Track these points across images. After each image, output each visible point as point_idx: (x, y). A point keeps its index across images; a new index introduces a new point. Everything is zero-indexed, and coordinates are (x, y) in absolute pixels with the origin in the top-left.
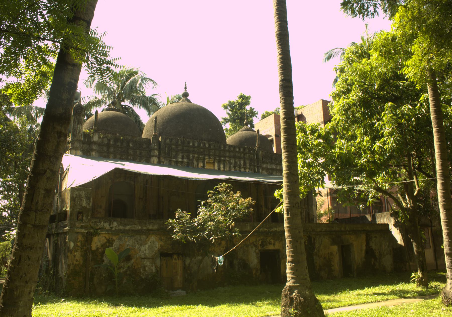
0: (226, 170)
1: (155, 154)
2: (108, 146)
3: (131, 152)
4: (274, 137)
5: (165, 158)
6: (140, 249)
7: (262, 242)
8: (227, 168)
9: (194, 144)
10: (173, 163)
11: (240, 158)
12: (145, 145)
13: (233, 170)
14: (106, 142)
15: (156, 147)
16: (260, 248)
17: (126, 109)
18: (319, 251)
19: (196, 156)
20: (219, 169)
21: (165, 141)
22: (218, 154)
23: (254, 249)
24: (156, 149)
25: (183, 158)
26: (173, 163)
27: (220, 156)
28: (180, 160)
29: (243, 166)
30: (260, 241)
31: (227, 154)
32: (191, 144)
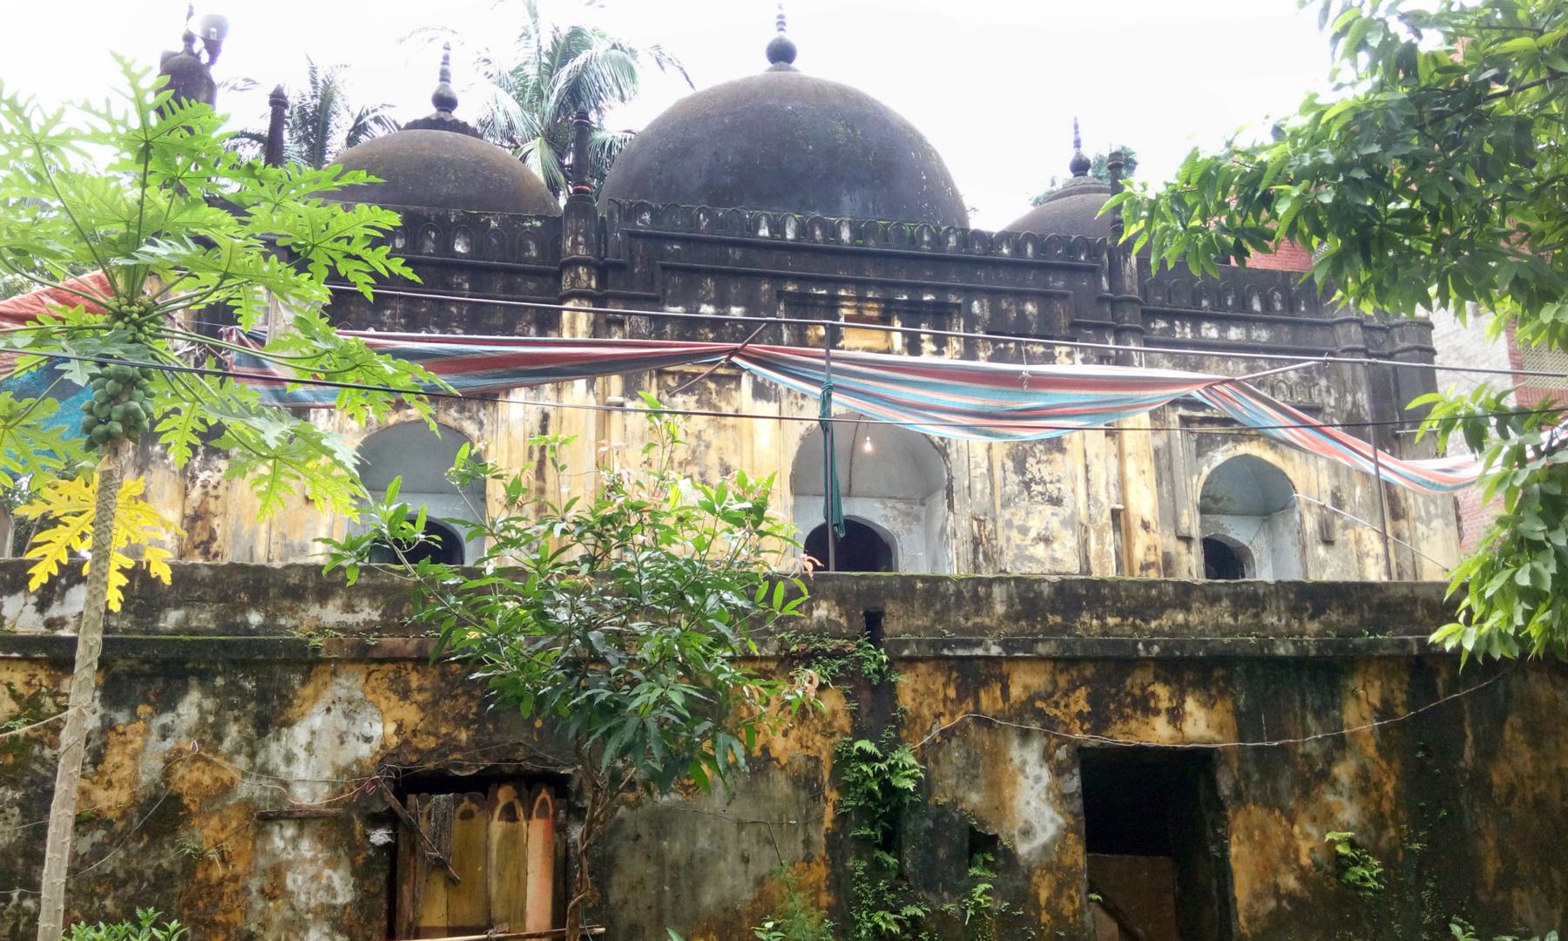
28: (707, 310)
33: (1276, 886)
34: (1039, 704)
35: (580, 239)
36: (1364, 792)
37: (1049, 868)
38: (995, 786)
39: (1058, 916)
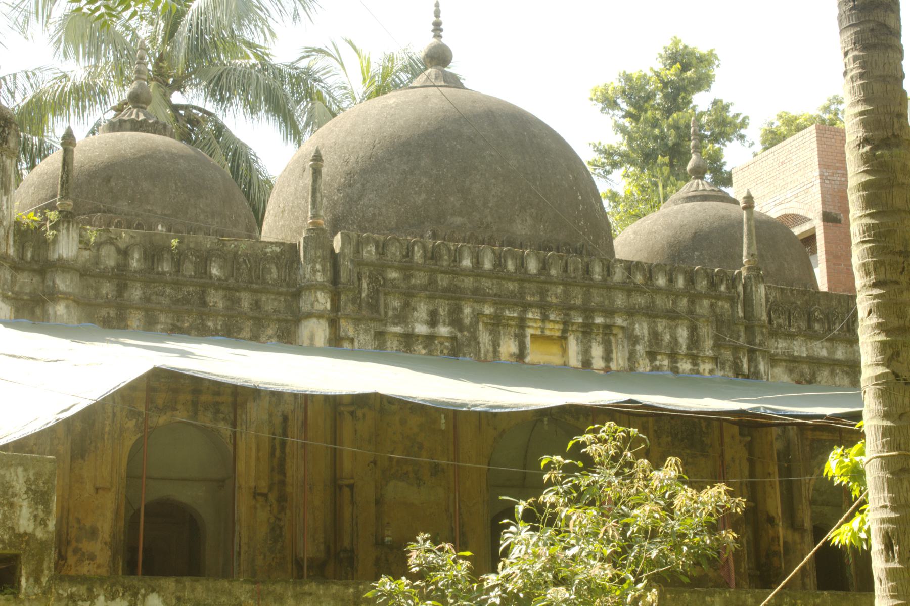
0: (613, 366)
1: (319, 307)
2: (121, 276)
3: (216, 299)
4: (817, 224)
5: (357, 321)
8: (619, 361)
9: (478, 263)
10: (392, 344)
11: (673, 316)
12: (274, 270)
13: (644, 365)
14: (111, 263)
15: (319, 277)
17: (188, 123)
19: (488, 310)
20: (587, 364)
21: (357, 251)
22: (579, 302)
24: (321, 287)
25: (433, 321)
26: (392, 344)
27: (588, 311)
28: (421, 329)
29: (689, 348)
31: (620, 300)
32: (467, 263)
35: (318, 267)
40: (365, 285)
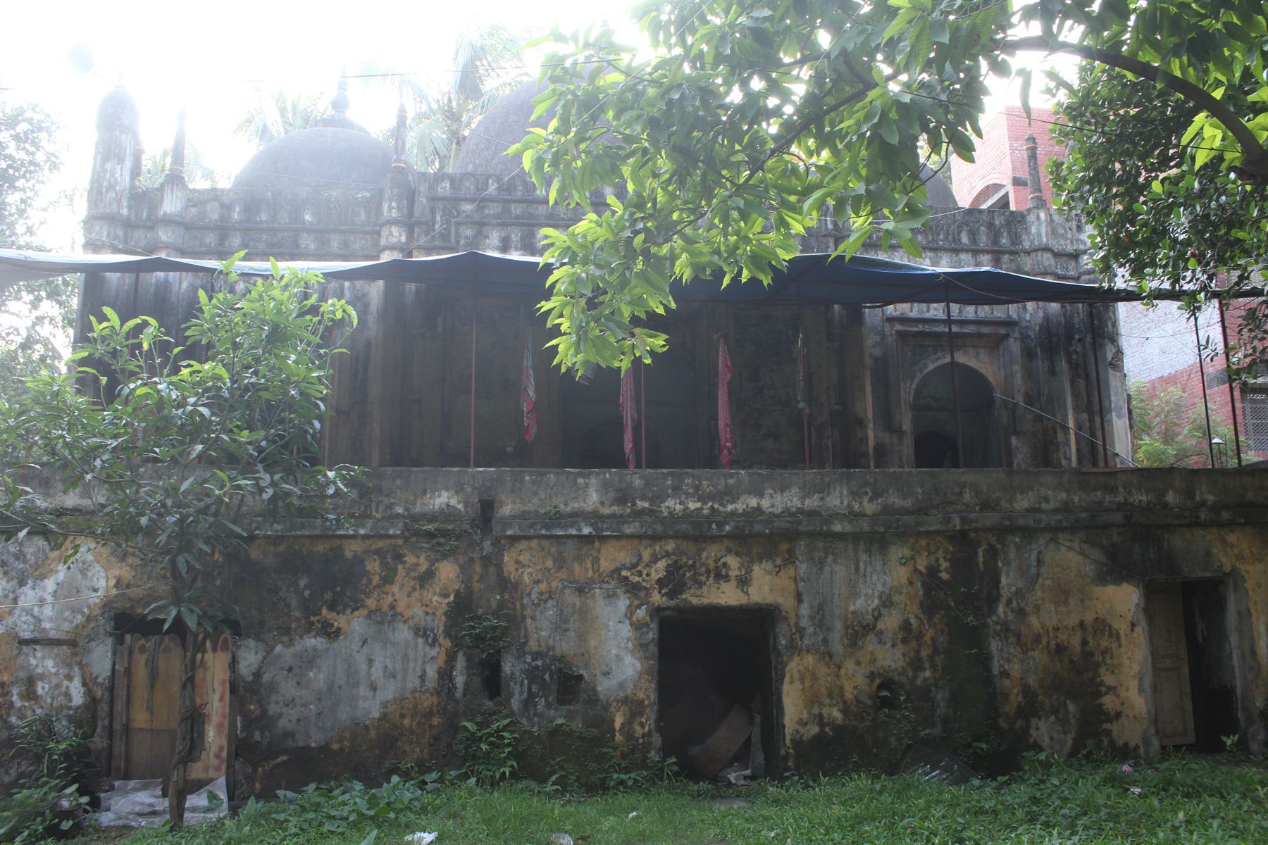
1: (393, 240)
4: (1010, 188)
6: (15, 600)
7: (668, 569)
14: (216, 216)
15: (394, 214)
16: (657, 598)
18: (1021, 612)
23: (623, 603)
24: (395, 222)
30: (662, 564)
33: (821, 716)
34: (624, 573)
35: (394, 204)
36: (904, 641)
37: (625, 700)
38: (582, 638)
39: (630, 736)
40: (438, 218)
